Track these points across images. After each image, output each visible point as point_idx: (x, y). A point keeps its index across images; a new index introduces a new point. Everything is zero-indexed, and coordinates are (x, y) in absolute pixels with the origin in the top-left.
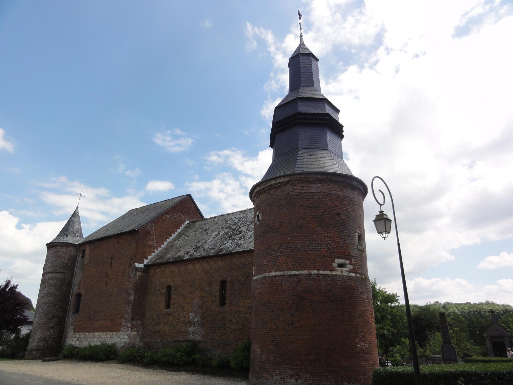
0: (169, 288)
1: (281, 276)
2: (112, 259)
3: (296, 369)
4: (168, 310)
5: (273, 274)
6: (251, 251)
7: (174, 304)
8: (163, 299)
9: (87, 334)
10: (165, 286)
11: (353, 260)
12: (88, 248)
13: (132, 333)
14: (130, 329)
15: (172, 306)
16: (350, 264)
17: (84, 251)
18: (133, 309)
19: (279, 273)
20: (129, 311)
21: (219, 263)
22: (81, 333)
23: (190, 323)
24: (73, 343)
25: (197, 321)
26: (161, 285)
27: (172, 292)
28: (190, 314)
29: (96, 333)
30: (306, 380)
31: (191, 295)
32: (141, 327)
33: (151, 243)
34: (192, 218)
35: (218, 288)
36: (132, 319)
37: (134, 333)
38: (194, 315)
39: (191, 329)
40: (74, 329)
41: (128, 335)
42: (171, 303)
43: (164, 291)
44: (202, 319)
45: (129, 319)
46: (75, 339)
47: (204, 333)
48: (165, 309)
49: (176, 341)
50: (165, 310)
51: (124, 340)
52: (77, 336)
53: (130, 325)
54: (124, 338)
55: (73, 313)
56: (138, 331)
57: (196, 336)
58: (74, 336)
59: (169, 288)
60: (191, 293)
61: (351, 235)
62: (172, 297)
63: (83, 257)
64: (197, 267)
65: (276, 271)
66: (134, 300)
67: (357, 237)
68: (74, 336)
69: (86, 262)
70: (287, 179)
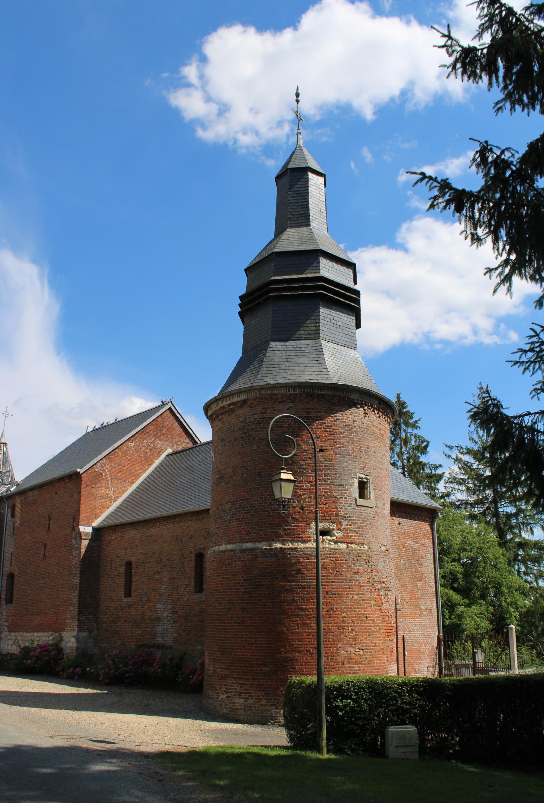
1: (231, 550)
2: (50, 519)
3: (247, 684)
4: (129, 599)
5: (223, 548)
6: (207, 511)
7: (136, 590)
9: (25, 634)
10: (124, 563)
11: (344, 522)
12: (18, 501)
13: (80, 634)
14: (76, 628)
15: (133, 594)
16: (339, 529)
17: (13, 508)
18: (80, 597)
19: (230, 547)
20: (75, 600)
22: (17, 634)
23: (158, 619)
24: (9, 647)
26: (118, 560)
27: (133, 571)
29: (35, 634)
30: (259, 699)
31: (157, 577)
32: (95, 626)
33: (104, 491)
34: (177, 444)
35: (192, 564)
36: (80, 613)
37: (85, 634)
38: (162, 606)
39: (159, 629)
40: (8, 627)
41: (74, 637)
42: (133, 589)
43: (122, 569)
44: (174, 613)
45: (75, 613)
46: (11, 642)
47: (176, 635)
48: (125, 597)
49: (141, 646)
50: (125, 600)
51: (70, 644)
52: (13, 638)
53: (76, 623)
55: (6, 603)
56: (90, 631)
57: (166, 639)
58: (9, 637)
60: (158, 572)
61: (343, 482)
62: (134, 579)
63: (13, 516)
65: (226, 544)
66: (81, 583)
67: (356, 485)
68: (9, 637)
69: (18, 524)
70: (243, 397)
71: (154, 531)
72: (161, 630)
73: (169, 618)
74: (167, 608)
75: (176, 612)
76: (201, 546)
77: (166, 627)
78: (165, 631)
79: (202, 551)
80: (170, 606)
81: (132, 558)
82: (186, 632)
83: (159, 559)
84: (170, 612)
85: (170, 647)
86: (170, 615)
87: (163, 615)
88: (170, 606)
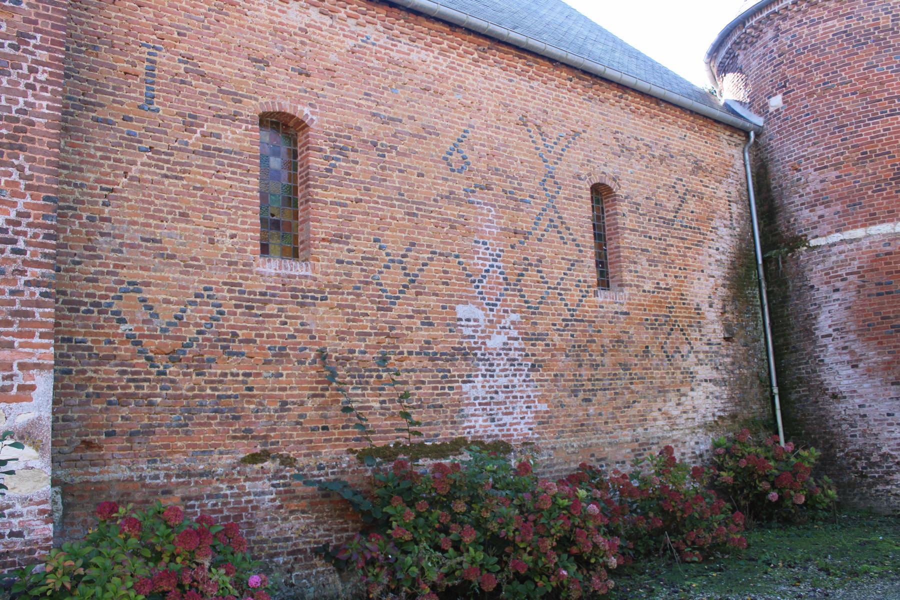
7: (340, 238)
10: (252, 108)
25: (506, 348)
28: (462, 311)
31: (452, 212)
38: (480, 314)
39: (476, 389)
47: (544, 407)
50: (272, 268)
53: (47, 353)
57: (507, 419)
60: (450, 196)
72: (481, 393)
73: (513, 354)
74: (506, 322)
75: (540, 337)
76: (606, 170)
77: (503, 381)
78: (501, 397)
79: (609, 183)
80: (515, 317)
81: (307, 110)
82: (581, 395)
83: (455, 157)
84: (514, 333)
86: (516, 344)
87: (490, 343)
88: (515, 317)
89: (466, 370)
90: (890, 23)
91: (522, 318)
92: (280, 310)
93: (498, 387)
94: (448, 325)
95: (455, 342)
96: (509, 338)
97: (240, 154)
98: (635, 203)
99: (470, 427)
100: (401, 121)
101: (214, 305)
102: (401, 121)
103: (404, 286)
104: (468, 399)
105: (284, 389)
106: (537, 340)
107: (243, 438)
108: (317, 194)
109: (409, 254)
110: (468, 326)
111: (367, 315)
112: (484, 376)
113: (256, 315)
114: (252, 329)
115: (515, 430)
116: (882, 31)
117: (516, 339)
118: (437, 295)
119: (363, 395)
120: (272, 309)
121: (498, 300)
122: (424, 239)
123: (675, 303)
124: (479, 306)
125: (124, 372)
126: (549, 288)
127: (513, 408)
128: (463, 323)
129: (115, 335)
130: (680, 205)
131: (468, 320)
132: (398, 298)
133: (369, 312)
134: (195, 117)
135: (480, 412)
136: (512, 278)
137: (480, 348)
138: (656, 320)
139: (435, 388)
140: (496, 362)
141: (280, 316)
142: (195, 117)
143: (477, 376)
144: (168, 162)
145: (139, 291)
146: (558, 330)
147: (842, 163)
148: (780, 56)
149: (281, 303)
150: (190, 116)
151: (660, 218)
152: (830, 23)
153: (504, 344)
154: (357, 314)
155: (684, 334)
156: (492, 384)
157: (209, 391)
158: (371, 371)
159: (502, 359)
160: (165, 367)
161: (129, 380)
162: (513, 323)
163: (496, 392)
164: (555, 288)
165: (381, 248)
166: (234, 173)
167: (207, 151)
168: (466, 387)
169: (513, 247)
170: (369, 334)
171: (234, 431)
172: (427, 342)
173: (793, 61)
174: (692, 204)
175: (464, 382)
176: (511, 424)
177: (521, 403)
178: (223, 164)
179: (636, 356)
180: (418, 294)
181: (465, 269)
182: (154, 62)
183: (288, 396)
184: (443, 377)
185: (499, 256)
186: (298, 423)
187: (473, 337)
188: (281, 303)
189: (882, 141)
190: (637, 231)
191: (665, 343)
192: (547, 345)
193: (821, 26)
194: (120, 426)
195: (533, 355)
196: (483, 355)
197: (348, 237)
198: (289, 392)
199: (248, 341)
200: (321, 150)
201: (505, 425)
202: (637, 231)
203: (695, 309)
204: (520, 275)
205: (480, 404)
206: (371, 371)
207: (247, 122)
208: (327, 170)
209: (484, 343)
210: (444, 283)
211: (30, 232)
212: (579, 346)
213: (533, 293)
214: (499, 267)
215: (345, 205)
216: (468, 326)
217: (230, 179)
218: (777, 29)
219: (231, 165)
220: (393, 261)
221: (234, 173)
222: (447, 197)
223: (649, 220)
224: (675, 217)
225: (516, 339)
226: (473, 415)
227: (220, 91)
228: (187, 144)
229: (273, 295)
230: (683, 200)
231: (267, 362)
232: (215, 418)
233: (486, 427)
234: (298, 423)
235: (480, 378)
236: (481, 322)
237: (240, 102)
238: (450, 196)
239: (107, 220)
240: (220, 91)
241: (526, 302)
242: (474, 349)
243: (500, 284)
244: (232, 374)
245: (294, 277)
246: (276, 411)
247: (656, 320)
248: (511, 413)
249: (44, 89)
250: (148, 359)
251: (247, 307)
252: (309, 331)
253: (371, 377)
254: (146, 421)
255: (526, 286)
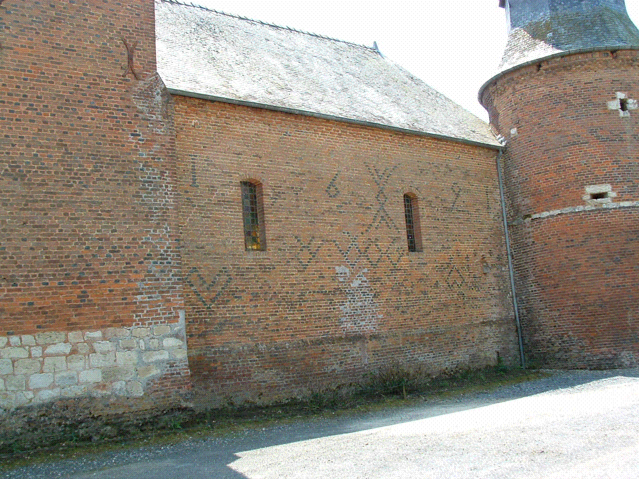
0: (252, 188)
8: (235, 217)
10: (237, 179)
21: (400, 152)
25: (360, 286)
38: (347, 270)
39: (347, 308)
41: (177, 336)
43: (235, 193)
47: (381, 316)
50: (250, 256)
51: (165, 356)
54: (160, 348)
57: (363, 323)
59: (252, 188)
64: (345, 145)
71: (318, 138)
77: (360, 304)
78: (359, 312)
84: (365, 279)
85: (374, 337)
86: (365, 284)
87: (352, 285)
88: (365, 270)
89: (341, 299)
90: (572, 92)
91: (368, 270)
92: (255, 275)
93: (357, 307)
94: (332, 277)
95: (335, 285)
96: (362, 282)
97: (234, 202)
98: (429, 201)
99: (345, 327)
100: (304, 174)
101: (227, 276)
102: (304, 174)
103: (310, 259)
104: (343, 313)
105: (259, 312)
106: (376, 281)
107: (243, 336)
108: (268, 217)
109: (311, 242)
110: (341, 277)
111: (293, 275)
112: (350, 301)
113: (245, 279)
114: (243, 285)
115: (367, 328)
116: (568, 96)
117: (365, 282)
118: (326, 262)
119: (294, 314)
120: (252, 275)
121: (356, 262)
122: (317, 234)
123: (453, 256)
124: (346, 266)
125: (194, 308)
126: (382, 253)
127: (366, 317)
128: (339, 275)
129: (190, 292)
130: (456, 199)
131: (341, 274)
132: (307, 265)
133: (294, 273)
134: (213, 187)
135: (349, 320)
136: (363, 250)
137: (347, 288)
138: (442, 266)
139: (327, 309)
140: (356, 294)
141: (255, 278)
142: (213, 187)
143: (347, 302)
144: (203, 210)
145: (198, 271)
146: (387, 275)
147: (548, 171)
148: (515, 105)
149: (255, 272)
150: (211, 187)
151: (444, 208)
152: (541, 89)
153: (360, 285)
154: (289, 275)
155: (459, 273)
156: (354, 305)
157: (228, 315)
158: (296, 302)
159: (359, 292)
160: (211, 305)
161: (197, 312)
162: (364, 273)
163: (356, 310)
164: (385, 253)
165: (298, 241)
166: (231, 212)
167: (219, 203)
168: (341, 308)
169: (362, 233)
170: (295, 284)
171: (239, 332)
172: (322, 286)
173: (522, 109)
174: (464, 196)
175: (340, 305)
176: (364, 326)
177: (369, 315)
178: (226, 208)
179: (431, 287)
180: (317, 262)
181: (338, 248)
182: (194, 163)
183: (261, 316)
184: (330, 303)
185: (355, 239)
186: (266, 328)
187: (344, 282)
188: (255, 272)
189: (568, 159)
190: (431, 217)
191: (448, 278)
192: (381, 284)
193: (537, 90)
194: (194, 332)
195: (375, 289)
196: (349, 291)
197: (282, 237)
198: (261, 314)
199: (243, 291)
200: (269, 195)
201: (361, 326)
202: (431, 217)
203: (466, 258)
204: (366, 248)
205: (349, 316)
206: (296, 302)
207: (235, 186)
208: (272, 205)
209: (349, 285)
210: (329, 256)
211: (172, 254)
212: (399, 283)
213: (375, 256)
214: (355, 245)
215: (281, 221)
216: (341, 277)
217: (229, 215)
218: (514, 89)
219: (229, 208)
220: (304, 247)
221: (231, 212)
222: (328, 211)
223: (438, 210)
224: (453, 206)
225: (365, 282)
226: (345, 322)
227: (223, 172)
228: (211, 200)
229: (252, 269)
230: (458, 195)
231: (251, 300)
232: (231, 327)
233: (352, 327)
234: (266, 328)
235: (348, 303)
236: (348, 274)
237: (231, 176)
238: (330, 211)
239: (183, 240)
240: (223, 172)
241: (370, 262)
242: (345, 288)
243: (357, 254)
244: (237, 307)
245: (260, 259)
246: (256, 323)
247: (442, 266)
248: (365, 320)
249: (171, 194)
250: (203, 301)
251: (241, 275)
252: (268, 284)
253: (296, 305)
254: (204, 330)
255: (370, 253)
